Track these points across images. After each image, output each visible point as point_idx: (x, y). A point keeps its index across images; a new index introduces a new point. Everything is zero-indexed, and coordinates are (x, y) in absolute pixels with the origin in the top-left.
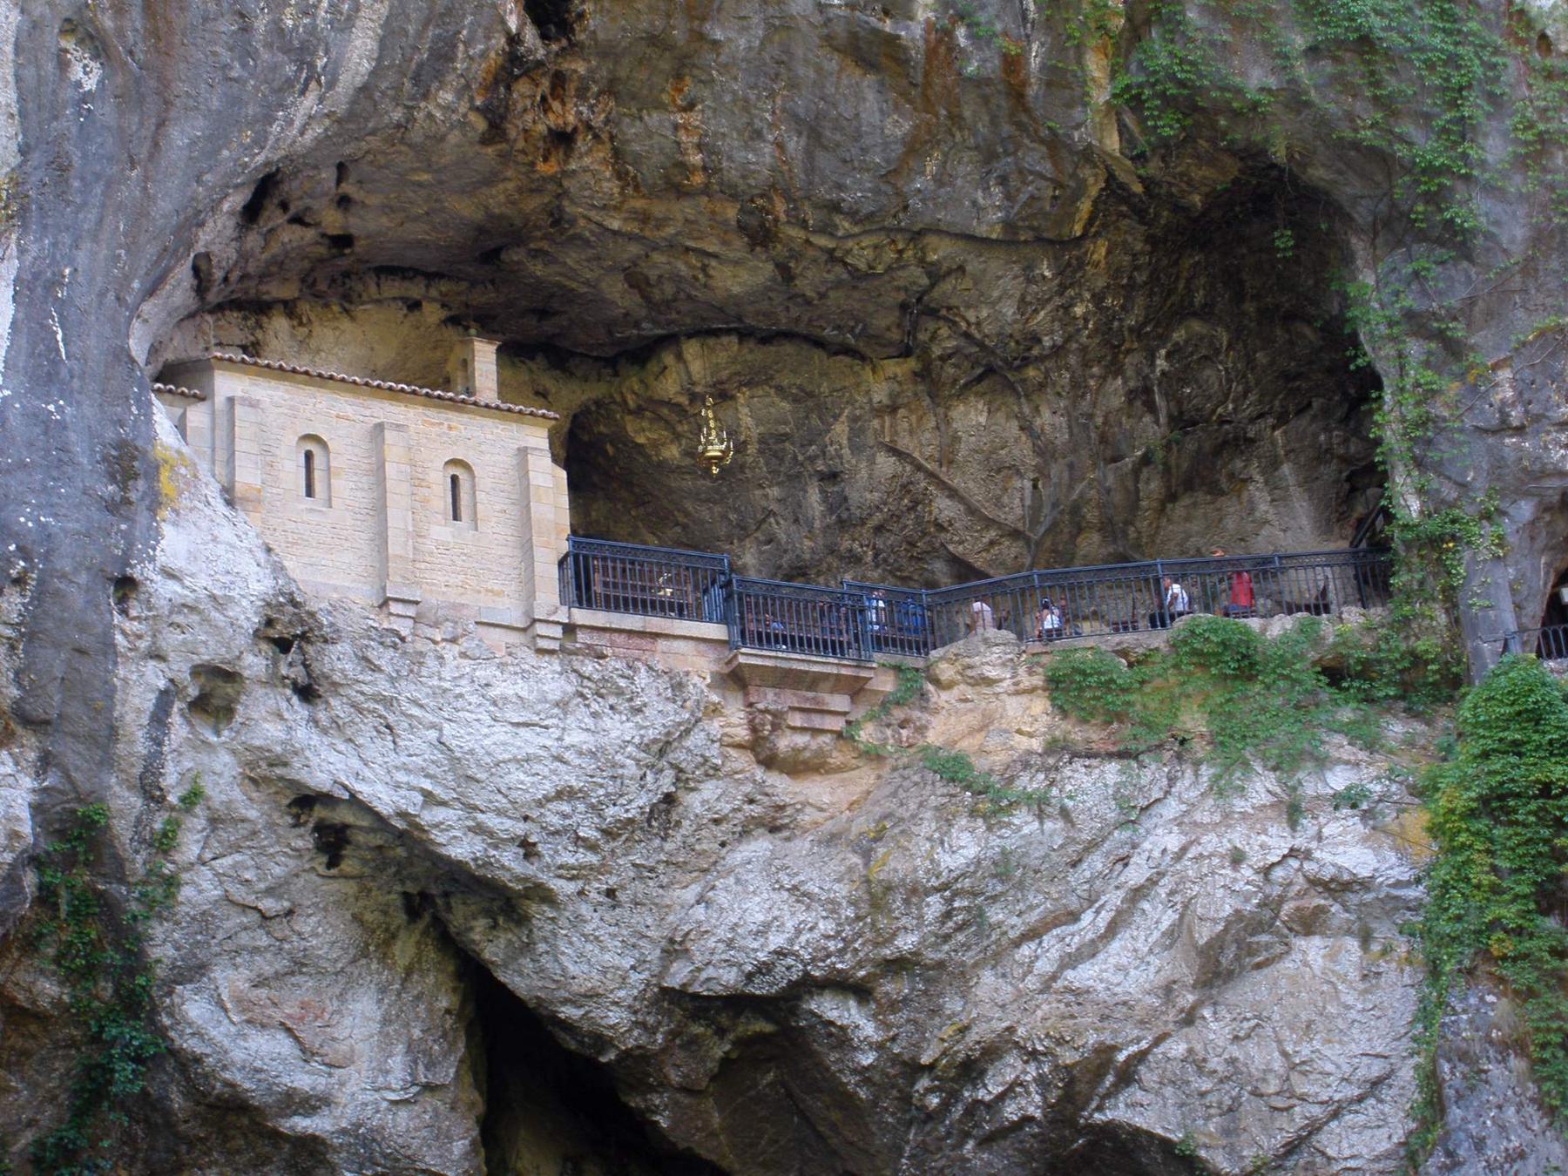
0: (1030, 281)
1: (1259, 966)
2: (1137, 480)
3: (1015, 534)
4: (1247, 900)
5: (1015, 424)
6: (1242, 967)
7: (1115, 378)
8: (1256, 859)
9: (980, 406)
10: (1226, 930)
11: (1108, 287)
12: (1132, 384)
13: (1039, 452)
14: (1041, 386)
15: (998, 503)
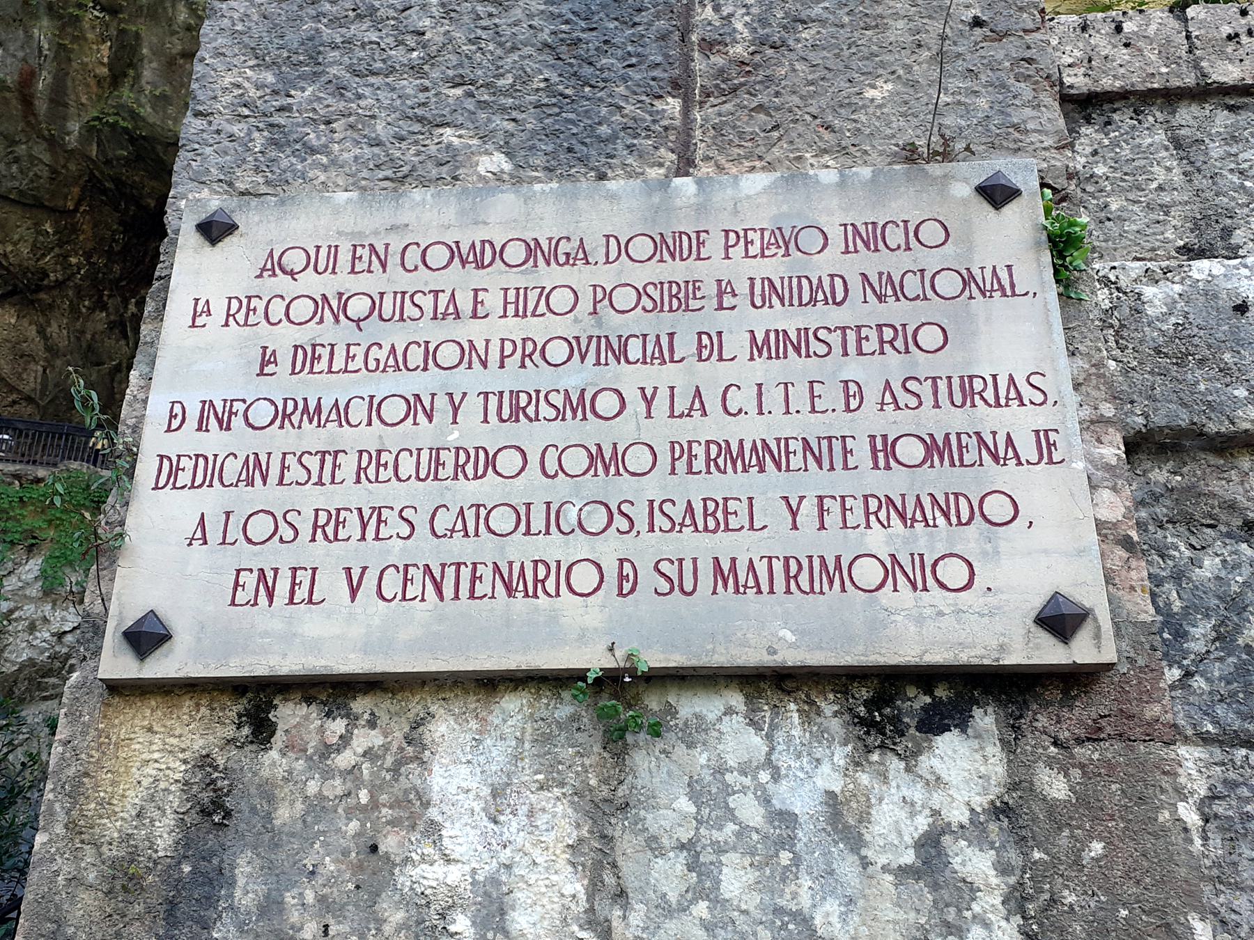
0: (39, 233)
1: (45, 699)
2: (112, 380)
3: (29, 399)
4: (42, 653)
5: (34, 327)
6: (32, 698)
7: (101, 311)
8: (55, 627)
9: (12, 311)
10: (19, 670)
11: (95, 249)
12: (112, 318)
13: (48, 349)
14: (51, 307)
15: (20, 378)
